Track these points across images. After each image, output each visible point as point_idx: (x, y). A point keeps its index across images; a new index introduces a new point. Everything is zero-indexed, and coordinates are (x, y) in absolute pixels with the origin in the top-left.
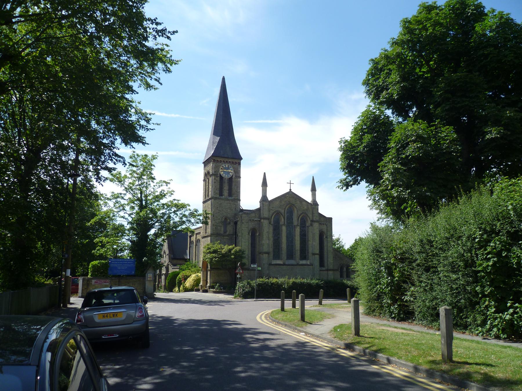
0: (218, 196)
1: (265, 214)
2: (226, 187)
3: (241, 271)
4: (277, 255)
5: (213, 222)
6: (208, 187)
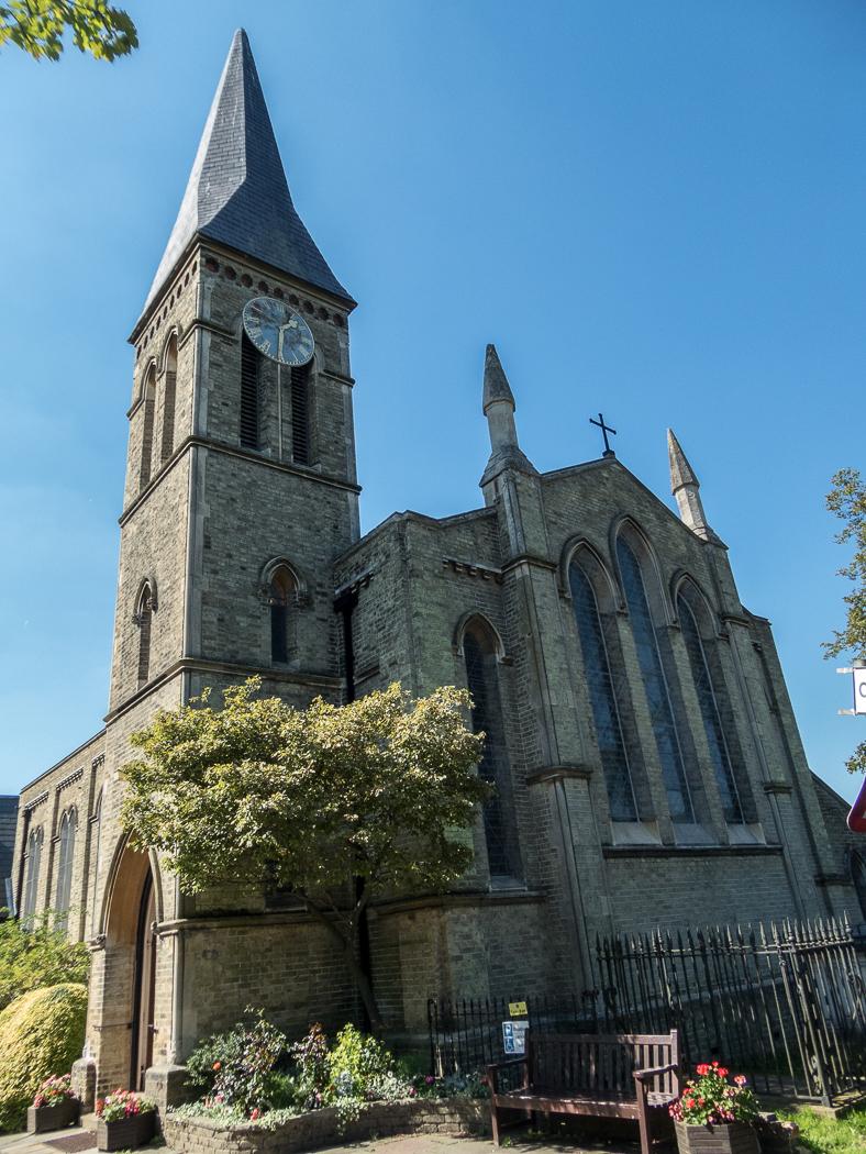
0: (234, 438)
5: (206, 579)
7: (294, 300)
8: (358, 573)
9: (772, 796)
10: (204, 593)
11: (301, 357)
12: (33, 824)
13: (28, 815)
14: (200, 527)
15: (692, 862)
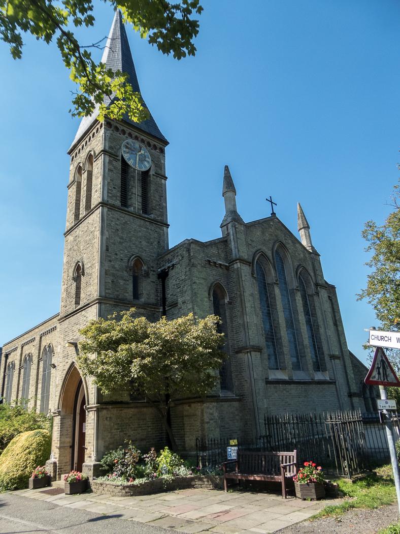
0: (118, 203)
2: (136, 190)
5: (107, 264)
7: (143, 141)
8: (169, 263)
9: (333, 360)
10: (106, 270)
11: (145, 166)
12: (9, 360)
13: (7, 356)
14: (104, 242)
15: (300, 387)
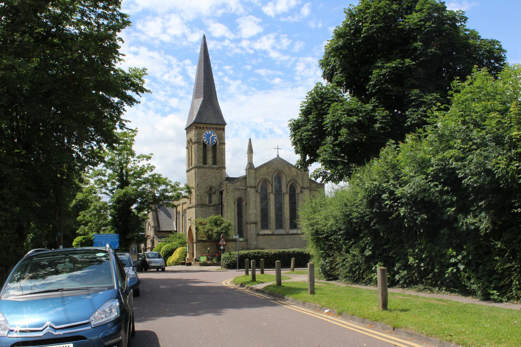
0: (202, 165)
1: (251, 182)
2: (210, 155)
3: (224, 243)
4: (265, 224)
6: (192, 156)
11: (214, 142)
12: (178, 210)
15: (278, 236)
